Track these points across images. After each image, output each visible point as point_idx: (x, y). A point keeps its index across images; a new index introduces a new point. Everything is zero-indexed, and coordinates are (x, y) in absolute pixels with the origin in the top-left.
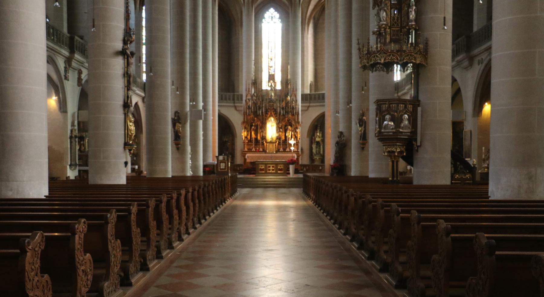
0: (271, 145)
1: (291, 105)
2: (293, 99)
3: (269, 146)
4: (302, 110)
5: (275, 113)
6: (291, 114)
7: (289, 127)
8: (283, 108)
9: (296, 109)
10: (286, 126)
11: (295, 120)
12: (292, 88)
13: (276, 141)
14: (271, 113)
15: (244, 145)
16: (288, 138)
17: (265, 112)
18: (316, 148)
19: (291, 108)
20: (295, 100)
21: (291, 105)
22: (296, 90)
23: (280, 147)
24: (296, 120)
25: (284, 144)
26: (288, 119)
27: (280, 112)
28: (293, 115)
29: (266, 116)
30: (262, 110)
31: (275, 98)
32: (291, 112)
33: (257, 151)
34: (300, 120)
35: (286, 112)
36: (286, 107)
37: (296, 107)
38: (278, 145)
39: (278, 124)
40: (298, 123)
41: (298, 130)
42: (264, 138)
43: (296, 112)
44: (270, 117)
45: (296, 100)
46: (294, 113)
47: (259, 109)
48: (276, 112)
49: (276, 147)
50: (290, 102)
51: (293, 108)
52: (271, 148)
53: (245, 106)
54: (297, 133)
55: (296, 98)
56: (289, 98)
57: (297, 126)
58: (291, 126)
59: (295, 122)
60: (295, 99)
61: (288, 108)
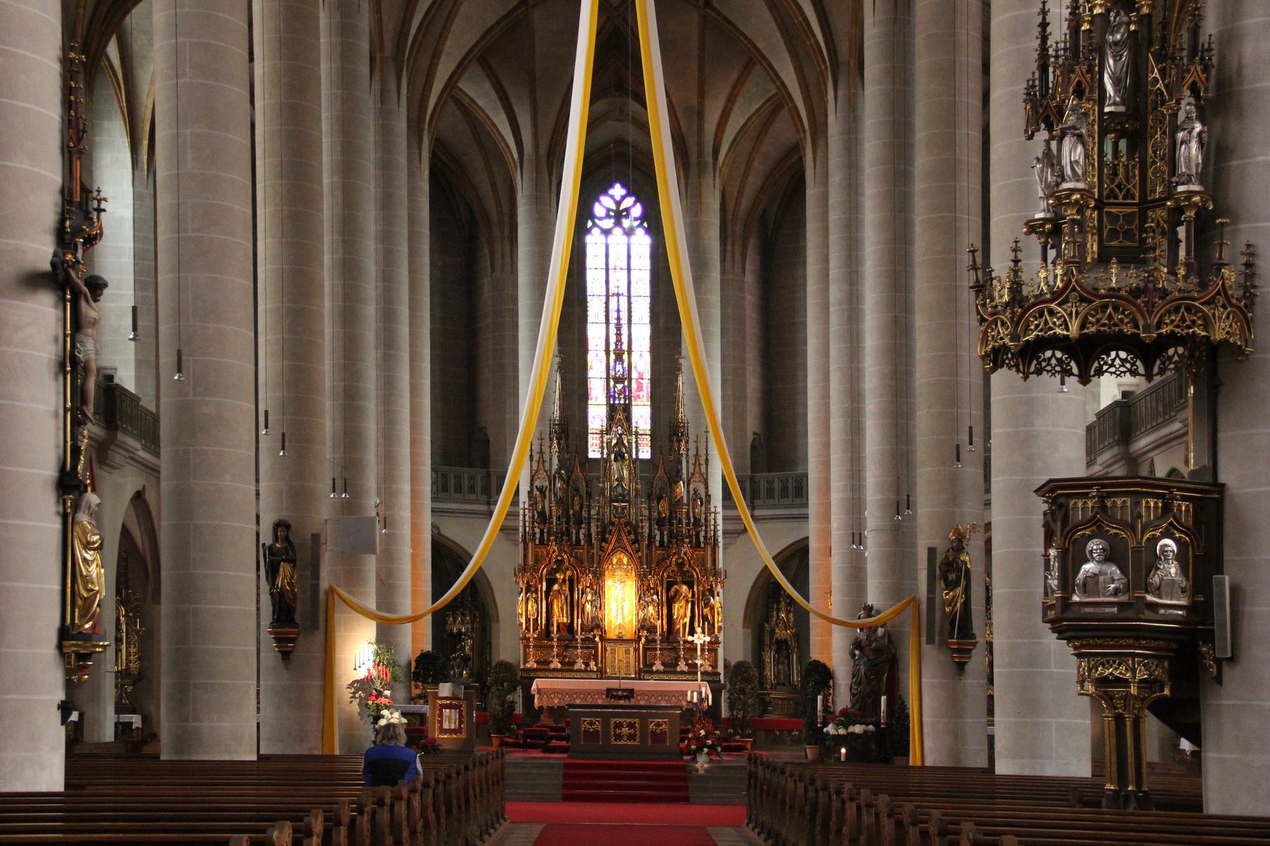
0: (620, 650)
1: (688, 513)
2: (695, 491)
3: (613, 652)
4: (724, 533)
5: (633, 537)
6: (691, 542)
7: (685, 588)
8: (660, 522)
9: (706, 527)
10: (670, 585)
11: (703, 564)
12: (692, 453)
13: (640, 638)
14: (619, 540)
15: (527, 647)
16: (680, 626)
17: (598, 533)
18: (777, 662)
19: (688, 525)
20: (703, 496)
21: (688, 513)
22: (707, 460)
23: (655, 658)
24: (709, 565)
25: (665, 646)
26: (680, 561)
27: (651, 537)
28: (698, 545)
29: (602, 549)
30: (589, 530)
31: (633, 485)
32: (690, 537)
33: (568, 667)
34: (720, 565)
35: (671, 535)
36: (670, 519)
37: (706, 520)
38: (645, 650)
39: (641, 578)
40: (716, 573)
41: (716, 601)
42: (596, 625)
43: (705, 537)
44: (613, 551)
45: (708, 496)
46: (702, 539)
47: (579, 523)
48: (636, 534)
49: (637, 659)
50: (685, 501)
51: (697, 523)
52: (622, 660)
53: (527, 511)
54: (712, 608)
55: (707, 487)
56: (681, 488)
57: (712, 586)
58: (691, 586)
59: (705, 572)
60: (702, 492)
61: (680, 522)
